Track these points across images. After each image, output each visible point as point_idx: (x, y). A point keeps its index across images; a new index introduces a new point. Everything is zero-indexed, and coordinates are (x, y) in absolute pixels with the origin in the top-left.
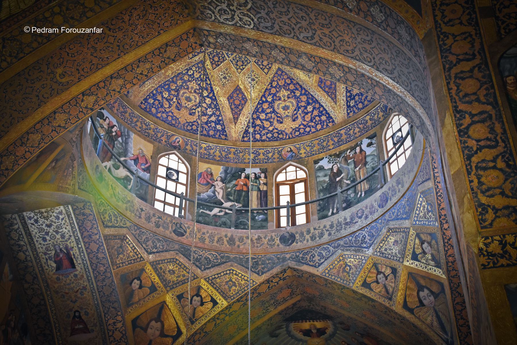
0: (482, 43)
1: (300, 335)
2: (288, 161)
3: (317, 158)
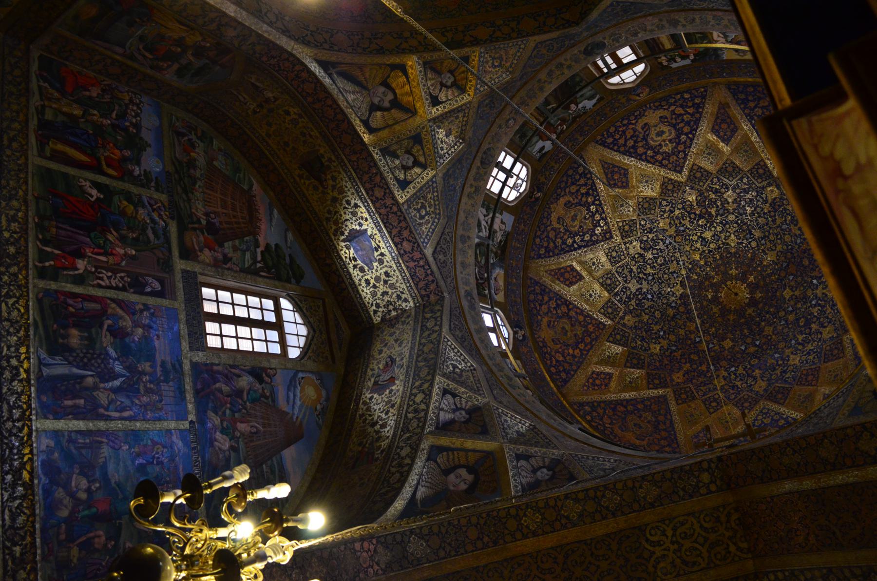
2: (638, 86)
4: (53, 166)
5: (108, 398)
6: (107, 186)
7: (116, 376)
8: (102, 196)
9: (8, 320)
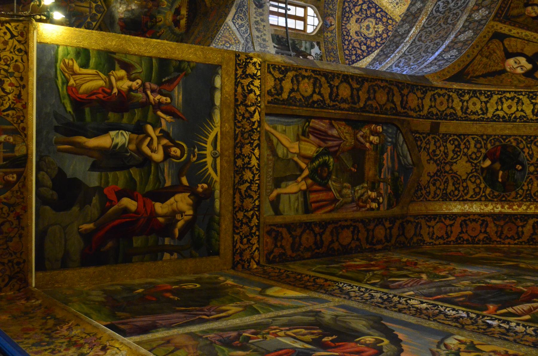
0: (412, 117)
1: (176, 5)
3: (321, 45)
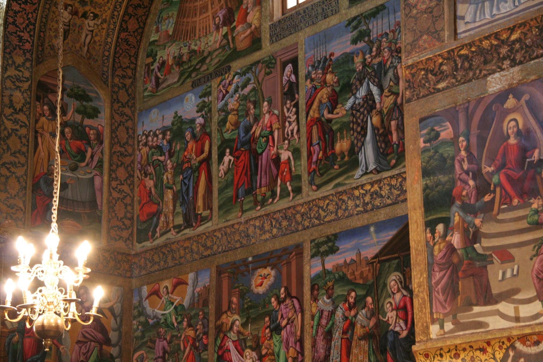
4: (216, 204)
5: (388, 97)
6: (219, 148)
7: (370, 93)
8: (228, 151)
9: (337, 213)
